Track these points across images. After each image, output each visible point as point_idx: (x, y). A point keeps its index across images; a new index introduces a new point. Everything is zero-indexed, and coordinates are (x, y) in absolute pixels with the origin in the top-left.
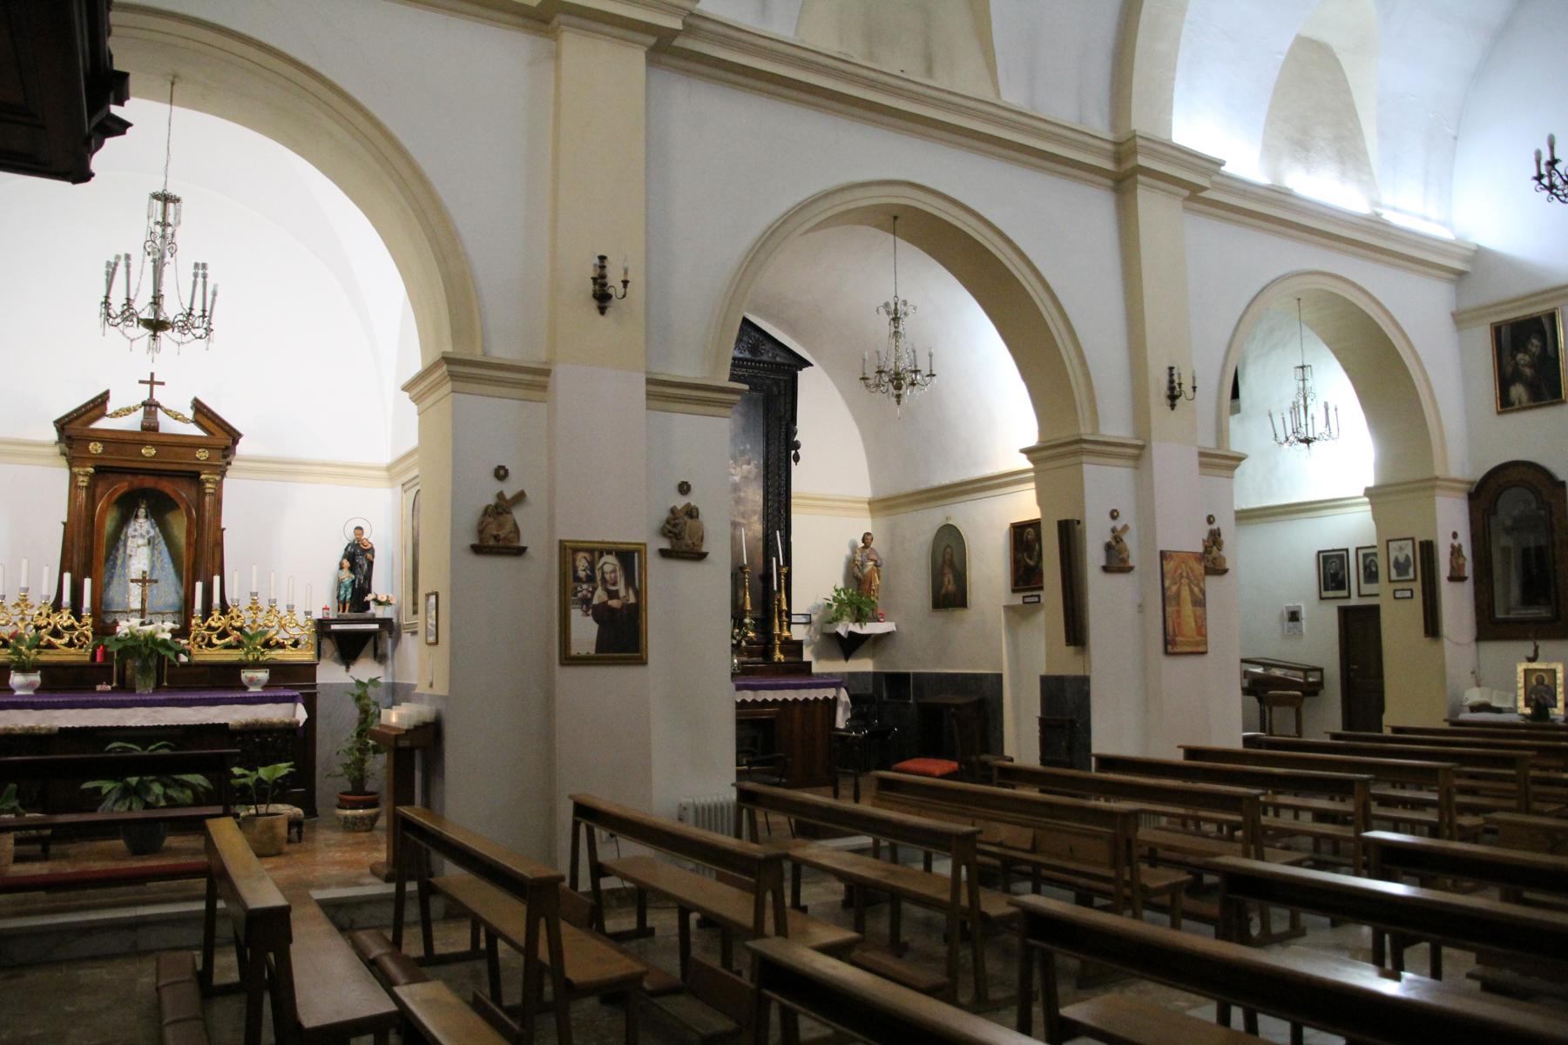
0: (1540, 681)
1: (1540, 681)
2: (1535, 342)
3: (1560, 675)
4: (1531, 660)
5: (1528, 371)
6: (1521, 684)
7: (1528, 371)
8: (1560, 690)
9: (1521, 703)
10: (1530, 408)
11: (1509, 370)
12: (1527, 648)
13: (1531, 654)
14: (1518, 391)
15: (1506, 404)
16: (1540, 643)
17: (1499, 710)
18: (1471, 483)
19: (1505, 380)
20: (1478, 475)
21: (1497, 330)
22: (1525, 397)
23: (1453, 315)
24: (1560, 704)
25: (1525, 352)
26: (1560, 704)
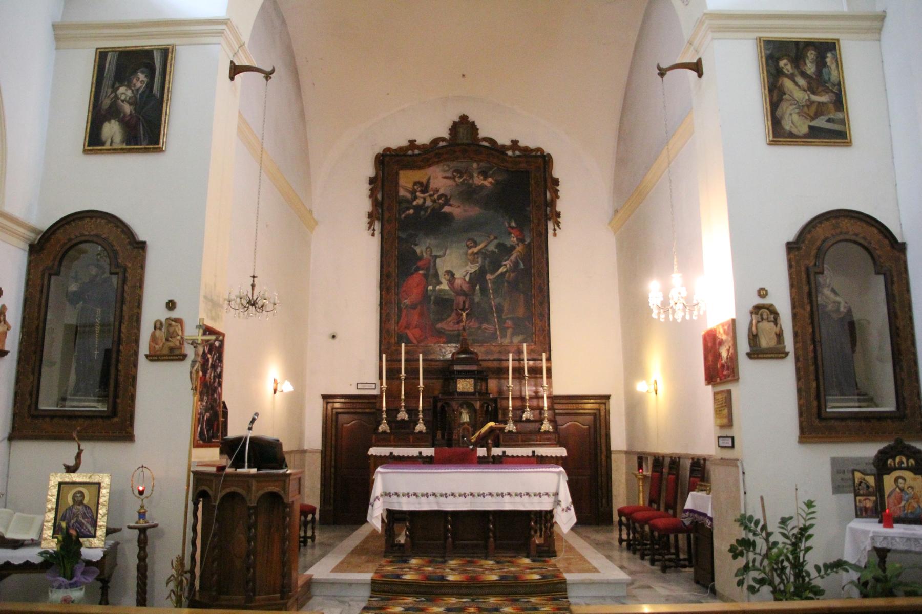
0: (78, 500)
1: (78, 500)
2: (142, 76)
3: (104, 491)
4: (70, 469)
5: (127, 109)
6: (52, 504)
7: (127, 109)
8: (102, 511)
9: (48, 533)
10: (122, 151)
11: (106, 103)
12: (66, 451)
13: (72, 463)
14: (112, 130)
15: (94, 141)
16: (86, 446)
17: (16, 544)
18: (34, 230)
19: (98, 117)
20: (45, 225)
21: (102, 55)
22: (118, 138)
23: (55, 26)
24: (101, 532)
25: (129, 87)
26: (101, 532)
